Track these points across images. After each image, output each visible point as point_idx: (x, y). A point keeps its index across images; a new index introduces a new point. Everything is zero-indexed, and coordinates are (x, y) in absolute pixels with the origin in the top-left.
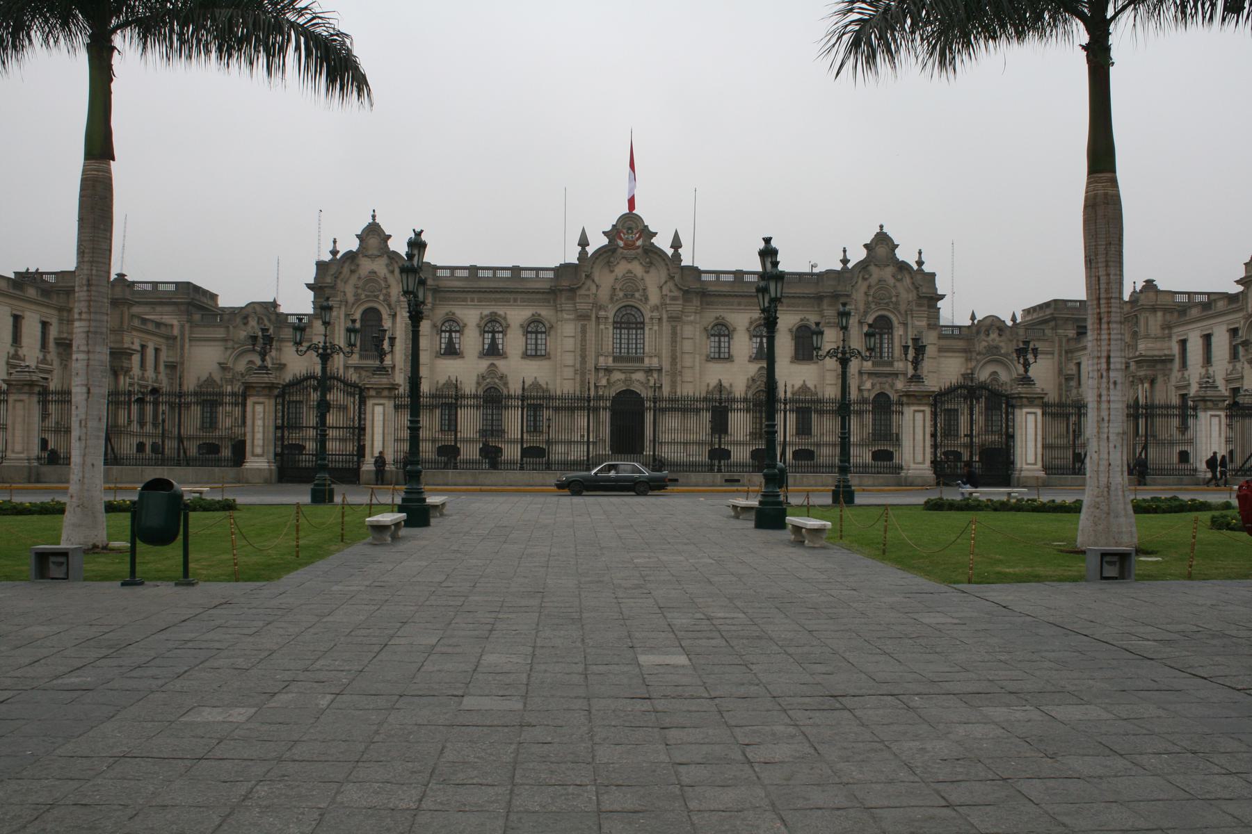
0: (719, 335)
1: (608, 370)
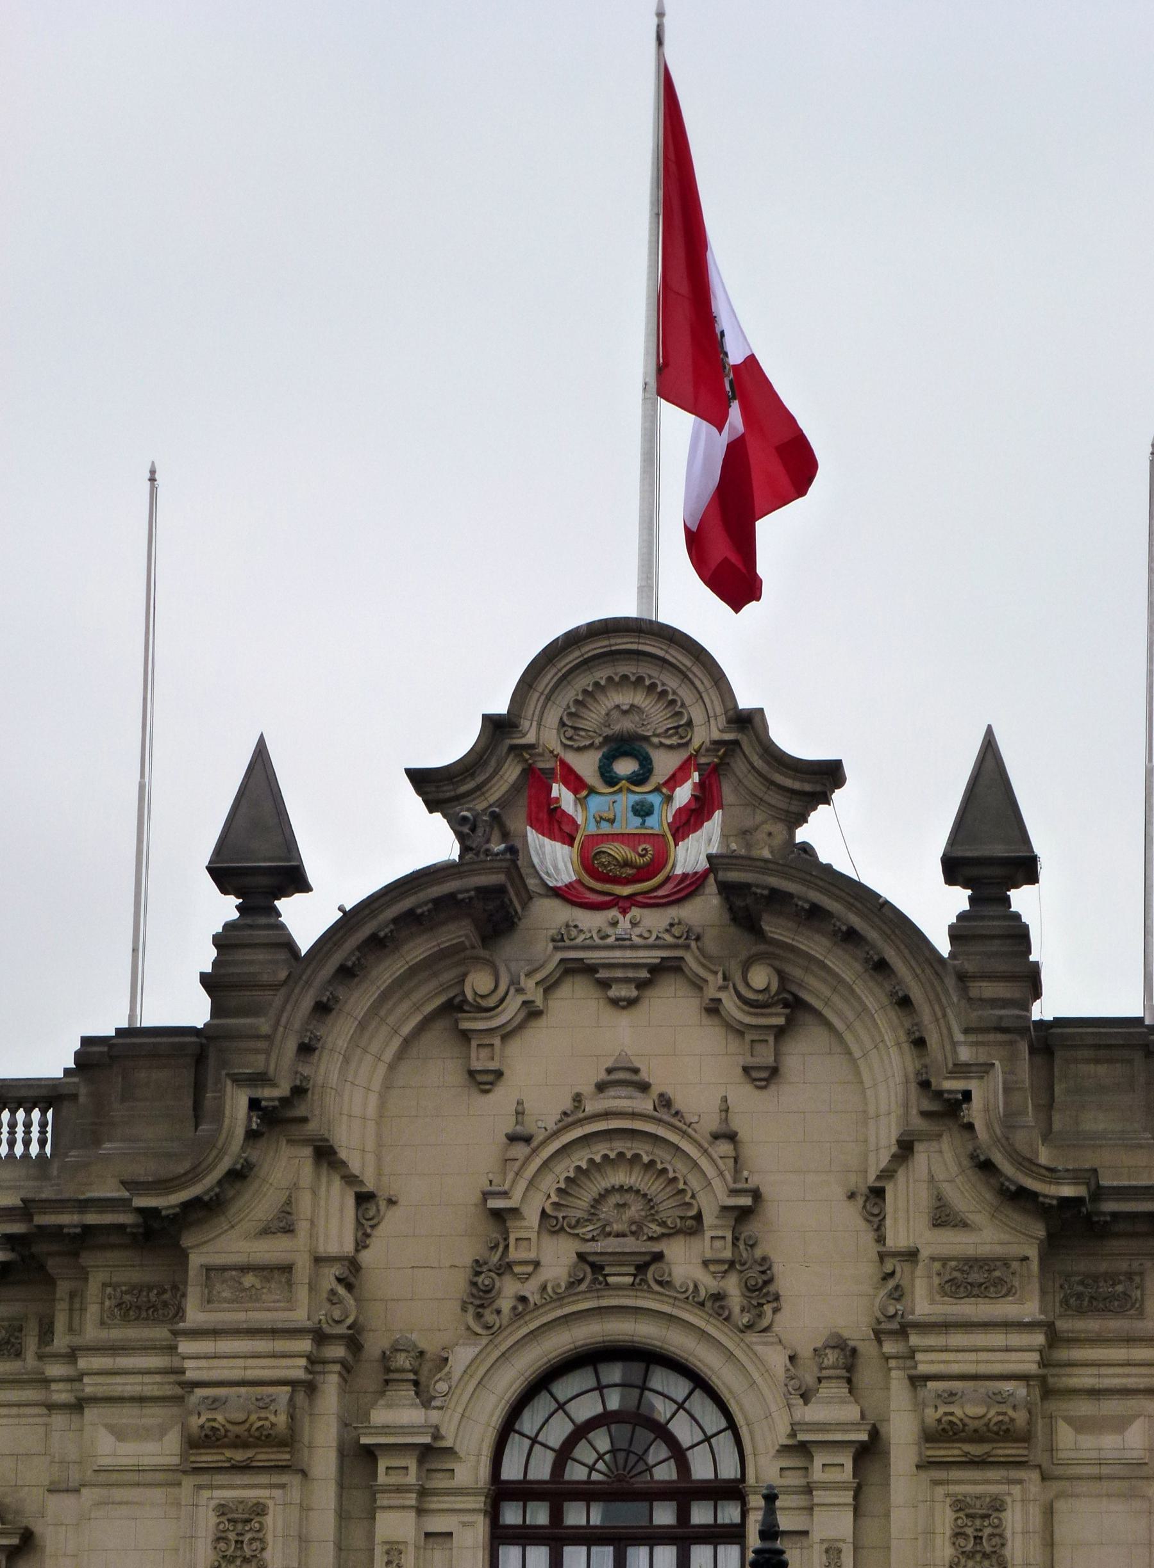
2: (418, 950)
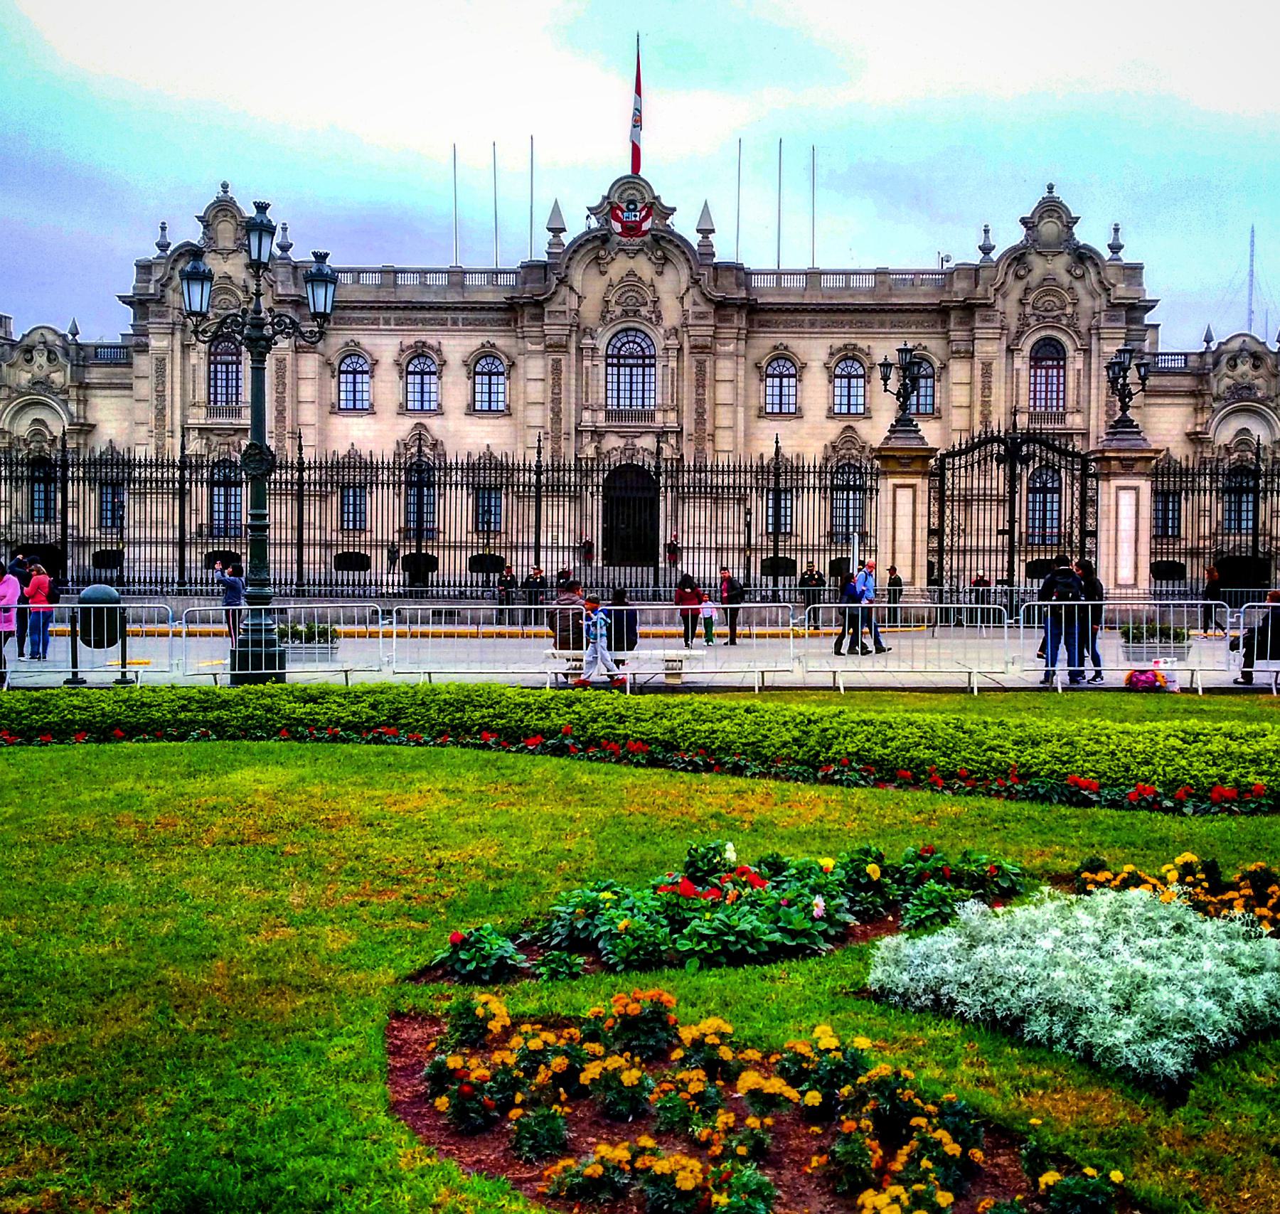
1: (598, 434)
2: (590, 246)
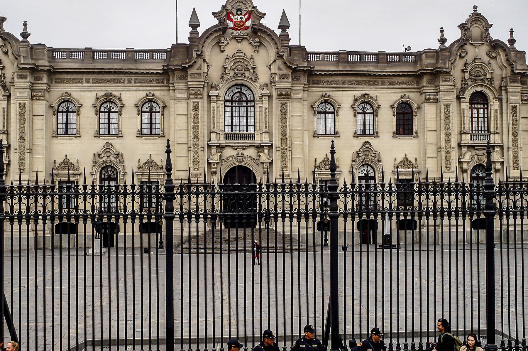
0: (325, 113)
1: (220, 147)
2: (216, 35)
